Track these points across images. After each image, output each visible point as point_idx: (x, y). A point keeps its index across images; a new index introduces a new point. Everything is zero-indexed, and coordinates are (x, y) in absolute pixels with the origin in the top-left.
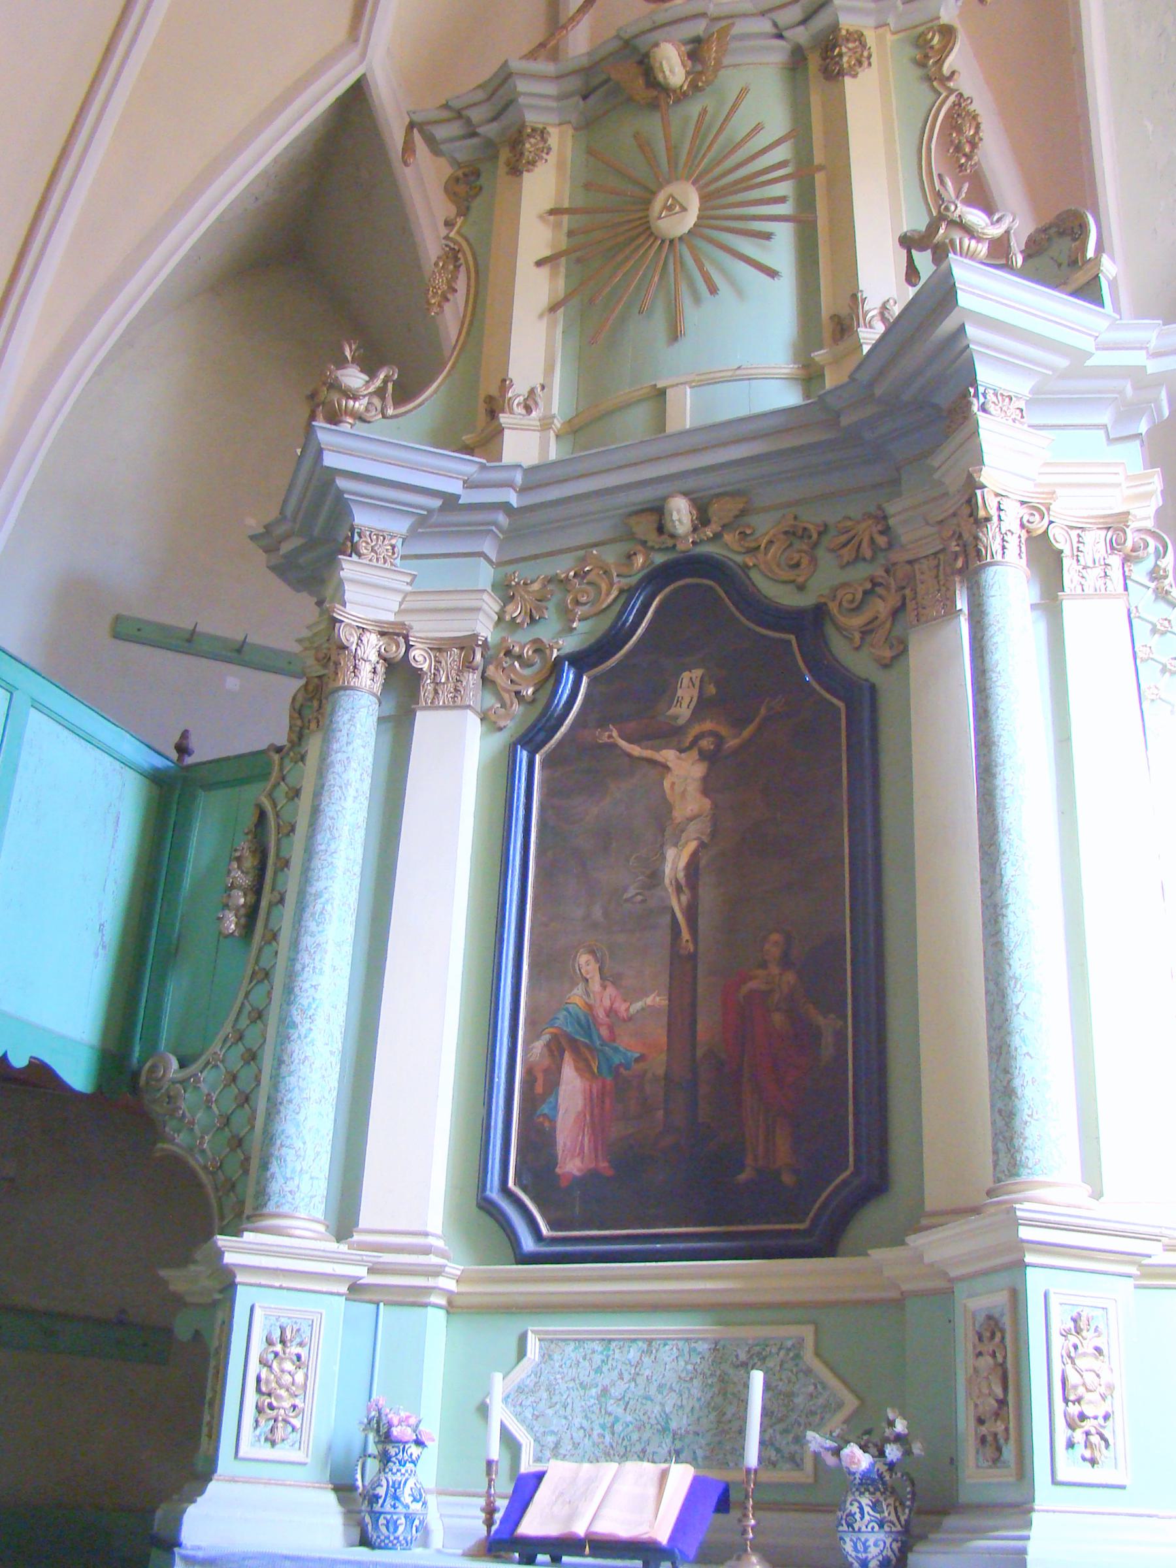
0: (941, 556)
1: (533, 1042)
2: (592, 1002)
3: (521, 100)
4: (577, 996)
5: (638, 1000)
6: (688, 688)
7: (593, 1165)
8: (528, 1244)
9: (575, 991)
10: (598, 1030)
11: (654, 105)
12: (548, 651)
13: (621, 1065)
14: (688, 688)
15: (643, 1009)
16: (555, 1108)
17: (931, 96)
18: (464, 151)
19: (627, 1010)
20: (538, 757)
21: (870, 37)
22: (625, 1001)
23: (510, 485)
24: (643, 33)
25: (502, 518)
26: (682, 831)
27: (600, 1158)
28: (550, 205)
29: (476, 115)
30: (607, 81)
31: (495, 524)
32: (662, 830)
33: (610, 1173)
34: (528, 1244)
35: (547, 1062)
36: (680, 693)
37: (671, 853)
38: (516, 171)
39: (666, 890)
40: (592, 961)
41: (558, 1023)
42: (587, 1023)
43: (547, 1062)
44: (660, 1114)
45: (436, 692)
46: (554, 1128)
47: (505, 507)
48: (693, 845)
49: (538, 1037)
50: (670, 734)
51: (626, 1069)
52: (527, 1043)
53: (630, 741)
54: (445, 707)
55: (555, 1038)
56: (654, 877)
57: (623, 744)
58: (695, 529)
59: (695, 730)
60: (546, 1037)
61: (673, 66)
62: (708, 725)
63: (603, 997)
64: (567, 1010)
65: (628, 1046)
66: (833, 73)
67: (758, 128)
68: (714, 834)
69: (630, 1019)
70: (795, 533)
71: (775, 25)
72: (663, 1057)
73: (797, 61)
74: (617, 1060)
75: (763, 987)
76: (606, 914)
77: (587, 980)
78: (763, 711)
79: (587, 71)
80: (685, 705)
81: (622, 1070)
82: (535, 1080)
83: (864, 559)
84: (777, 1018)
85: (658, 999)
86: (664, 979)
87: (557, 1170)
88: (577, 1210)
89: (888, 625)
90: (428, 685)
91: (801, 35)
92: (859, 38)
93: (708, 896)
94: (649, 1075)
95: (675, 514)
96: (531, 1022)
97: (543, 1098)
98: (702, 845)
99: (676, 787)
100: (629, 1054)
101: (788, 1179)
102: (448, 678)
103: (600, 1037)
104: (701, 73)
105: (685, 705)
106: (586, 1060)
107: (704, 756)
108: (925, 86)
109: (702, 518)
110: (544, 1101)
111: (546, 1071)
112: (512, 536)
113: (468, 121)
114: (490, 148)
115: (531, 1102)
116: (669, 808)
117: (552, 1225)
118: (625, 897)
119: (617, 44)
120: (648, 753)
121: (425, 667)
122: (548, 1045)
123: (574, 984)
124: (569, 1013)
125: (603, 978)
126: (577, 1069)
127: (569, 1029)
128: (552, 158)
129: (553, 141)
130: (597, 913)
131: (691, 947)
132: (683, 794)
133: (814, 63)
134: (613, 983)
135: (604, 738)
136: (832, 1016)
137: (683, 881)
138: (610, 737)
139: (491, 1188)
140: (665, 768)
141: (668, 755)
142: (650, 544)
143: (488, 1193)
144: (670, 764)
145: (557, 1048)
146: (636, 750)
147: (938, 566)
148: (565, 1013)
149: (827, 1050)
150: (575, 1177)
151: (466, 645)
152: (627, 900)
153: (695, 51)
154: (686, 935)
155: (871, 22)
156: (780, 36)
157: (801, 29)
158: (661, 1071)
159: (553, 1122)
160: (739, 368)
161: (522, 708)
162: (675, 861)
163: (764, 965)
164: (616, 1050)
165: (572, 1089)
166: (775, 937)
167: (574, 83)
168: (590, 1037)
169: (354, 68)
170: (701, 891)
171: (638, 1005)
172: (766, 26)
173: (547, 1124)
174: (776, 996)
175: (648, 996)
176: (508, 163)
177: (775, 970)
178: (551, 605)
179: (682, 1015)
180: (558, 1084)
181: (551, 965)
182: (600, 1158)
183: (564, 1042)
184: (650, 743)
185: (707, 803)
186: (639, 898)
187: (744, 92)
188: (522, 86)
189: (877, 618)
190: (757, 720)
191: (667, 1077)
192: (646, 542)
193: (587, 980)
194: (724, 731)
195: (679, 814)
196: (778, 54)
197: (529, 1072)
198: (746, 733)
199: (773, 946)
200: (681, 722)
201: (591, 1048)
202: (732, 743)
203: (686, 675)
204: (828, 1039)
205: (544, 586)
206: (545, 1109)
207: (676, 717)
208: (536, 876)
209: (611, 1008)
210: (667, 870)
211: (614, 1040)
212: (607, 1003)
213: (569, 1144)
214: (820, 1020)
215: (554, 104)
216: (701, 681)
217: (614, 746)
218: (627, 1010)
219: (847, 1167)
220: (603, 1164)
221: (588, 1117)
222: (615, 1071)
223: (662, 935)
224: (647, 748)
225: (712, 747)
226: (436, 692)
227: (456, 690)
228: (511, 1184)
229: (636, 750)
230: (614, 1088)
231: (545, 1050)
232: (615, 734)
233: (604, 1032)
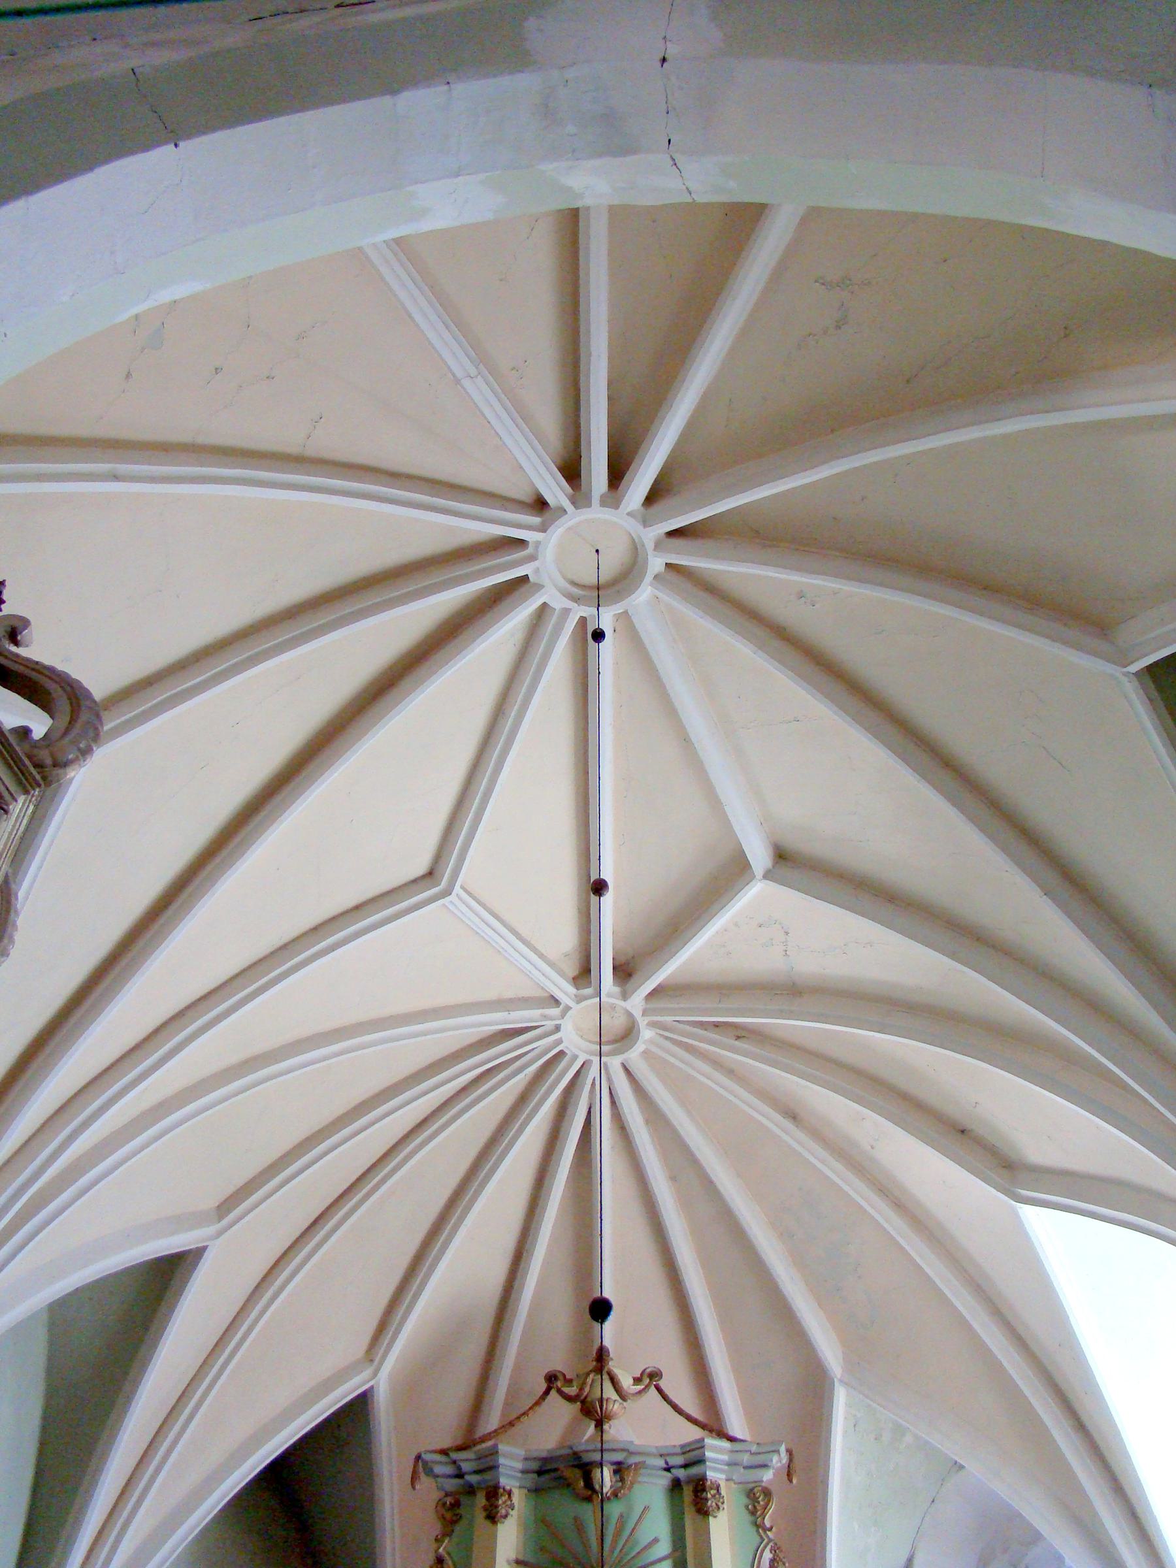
3: (501, 1470)
11: (589, 1499)
17: (758, 1539)
18: (452, 1484)
21: (723, 1484)
24: (587, 1451)
28: (513, 1555)
29: (466, 1467)
30: (556, 1470)
38: (492, 1517)
61: (606, 1478)
66: (703, 1511)
67: (656, 1540)
71: (667, 1463)
73: (676, 1485)
79: (545, 1460)
91: (681, 1473)
92: (718, 1488)
104: (622, 1487)
108: (754, 1529)
113: (459, 1468)
114: (471, 1490)
119: (568, 1451)
128: (514, 1513)
129: (516, 1499)
133: (688, 1492)
153: (619, 1469)
155: (723, 1476)
156: (668, 1469)
157: (682, 1470)
167: (535, 1466)
169: (364, 1384)
172: (661, 1463)
176: (485, 1508)
187: (646, 1509)
188: (502, 1460)
196: (664, 1480)
215: (520, 1475)
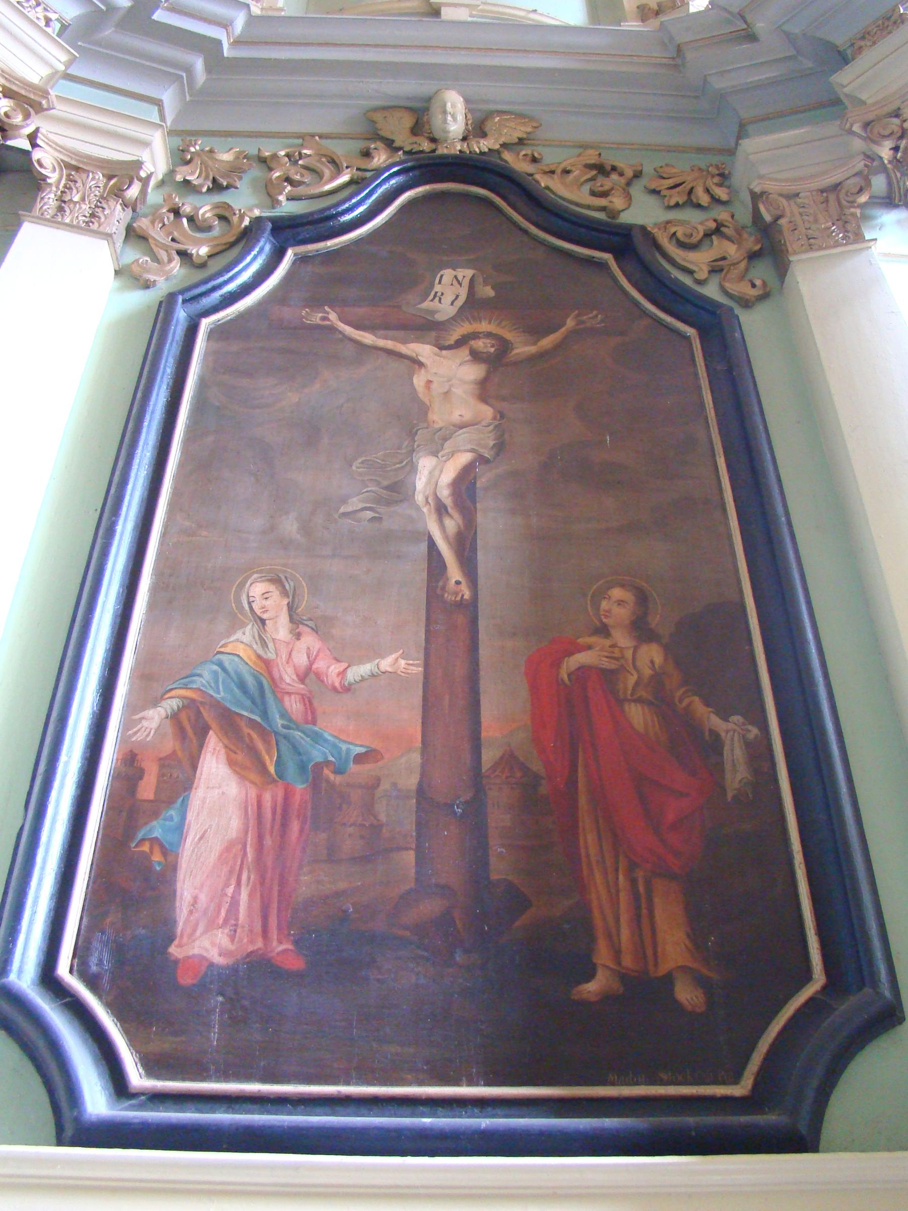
0: (832, 197)
1: (144, 708)
2: (271, 655)
4: (241, 644)
5: (361, 662)
6: (449, 290)
7: (259, 944)
8: (97, 1101)
9: (238, 635)
10: (281, 701)
12: (235, 219)
13: (327, 763)
14: (449, 290)
15: (373, 675)
16: (180, 829)
19: (343, 673)
20: (206, 324)
22: (338, 660)
23: (225, 25)
25: (199, 65)
26: (445, 439)
27: (274, 934)
31: (189, 70)
32: (412, 434)
33: (296, 963)
34: (97, 1101)
35: (170, 745)
36: (437, 288)
37: (425, 464)
39: (418, 509)
40: (275, 593)
41: (198, 682)
42: (261, 686)
43: (170, 745)
44: (410, 857)
45: (61, 209)
46: (174, 868)
47: (209, 48)
48: (464, 458)
49: (155, 702)
50: (427, 328)
51: (338, 771)
52: (131, 708)
53: (357, 327)
54: (71, 227)
55: (190, 705)
56: (397, 491)
57: (348, 330)
58: (464, 139)
59: (466, 328)
60: (171, 704)
62: (484, 326)
63: (293, 652)
64: (220, 664)
65: (340, 734)
68: (500, 447)
69: (347, 689)
70: (601, 169)
72: (416, 758)
74: (317, 754)
75: (606, 664)
76: (306, 529)
77: (263, 622)
78: (570, 323)
80: (448, 299)
81: (326, 771)
82: (140, 774)
83: (698, 206)
84: (637, 716)
85: (402, 662)
86: (416, 633)
87: (173, 950)
88: (214, 1036)
89: (743, 265)
90: (50, 199)
93: (494, 523)
94: (385, 785)
95: (449, 105)
96: (143, 676)
97: (155, 809)
98: (481, 459)
99: (434, 386)
100: (344, 747)
101: (687, 994)
102: (83, 199)
103: (284, 715)
105: (448, 299)
106: (252, 750)
107: (476, 356)
109: (477, 129)
110: (156, 815)
111: (164, 763)
112: (197, 100)
115: (126, 813)
116: (424, 410)
117: (153, 1065)
118: (342, 510)
120: (389, 344)
121: (53, 178)
122: (174, 717)
123: (236, 624)
124: (224, 669)
125: (294, 619)
126: (232, 763)
127: (221, 696)
130: (290, 526)
131: (467, 595)
132: (447, 394)
134: (315, 630)
135: (316, 318)
136: (737, 718)
137: (448, 502)
138: (325, 319)
139: (20, 971)
140: (417, 363)
141: (423, 350)
142: (396, 144)
143: (12, 977)
144: (420, 358)
145: (192, 726)
146: (367, 338)
147: (827, 201)
148: (215, 667)
149: (737, 772)
150: (212, 965)
151: (121, 175)
152: (345, 515)
154: (454, 573)
158: (412, 782)
159: (170, 854)
160: (535, 11)
161: (184, 271)
162: (433, 475)
163: (603, 630)
164: (317, 738)
165: (218, 800)
166: (617, 593)
168: (265, 714)
170: (480, 518)
171: (365, 669)
173: (157, 857)
174: (632, 680)
175: (383, 657)
177: (623, 640)
178: (247, 178)
179: (450, 691)
180: (187, 785)
181: (194, 591)
182: (274, 934)
183: (208, 715)
184: (391, 333)
185: (487, 412)
186: (369, 514)
189: (724, 258)
190: (563, 329)
191: (421, 791)
192: (393, 141)
193: (263, 622)
194: (508, 336)
195: (438, 417)
197: (130, 761)
198: (547, 342)
199: (618, 605)
200: (439, 317)
201: (264, 733)
202: (523, 349)
203: (448, 274)
204: (735, 755)
205: (237, 158)
206: (157, 829)
207: (433, 312)
208: (181, 465)
209: (309, 669)
210: (421, 483)
211: (314, 723)
212: (301, 659)
213: (203, 898)
214: (715, 722)
216: (472, 281)
217: (332, 329)
218: (343, 673)
219: (807, 976)
220: (280, 947)
221: (250, 851)
222: (315, 775)
223: (415, 572)
224: (386, 338)
225: (492, 350)
226: (61, 209)
227: (93, 215)
228: (63, 969)
229: (367, 338)
230: (307, 803)
231: (169, 729)
232: (333, 316)
233: (294, 706)
